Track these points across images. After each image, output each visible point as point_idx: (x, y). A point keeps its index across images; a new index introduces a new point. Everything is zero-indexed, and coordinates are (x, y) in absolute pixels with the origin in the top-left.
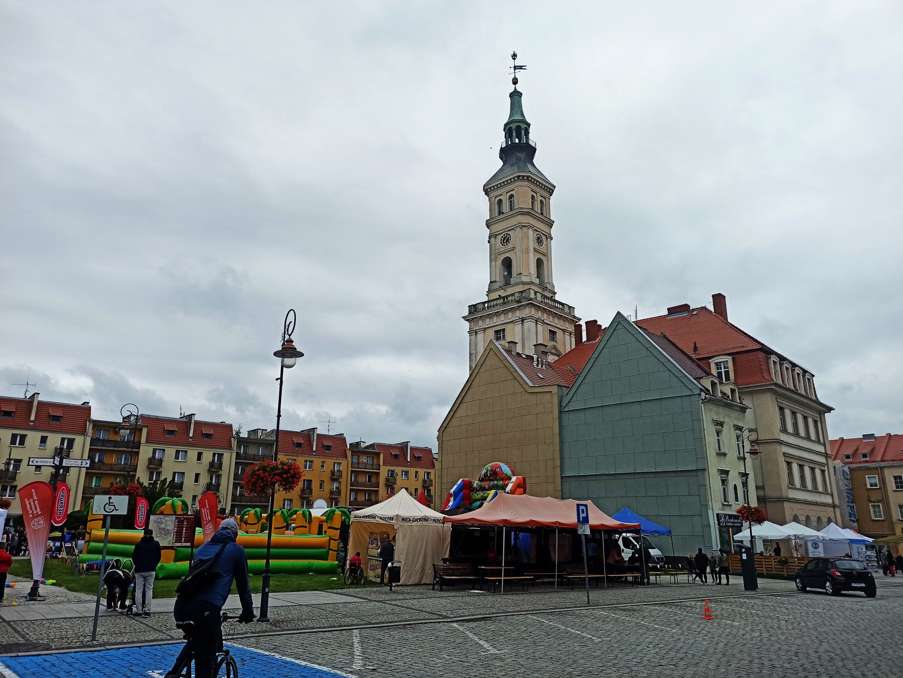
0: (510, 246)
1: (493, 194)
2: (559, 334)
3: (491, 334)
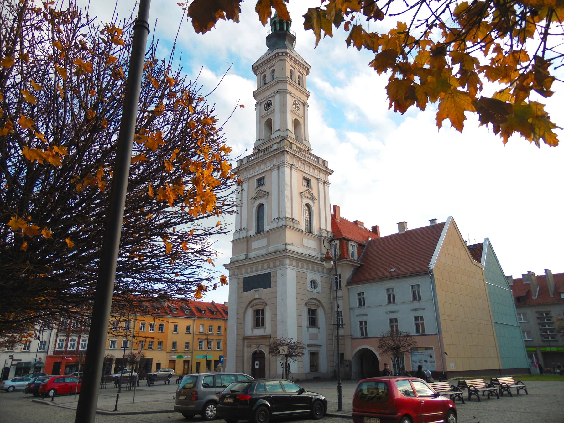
0: (271, 109)
1: (258, 72)
2: (314, 182)
3: (254, 182)
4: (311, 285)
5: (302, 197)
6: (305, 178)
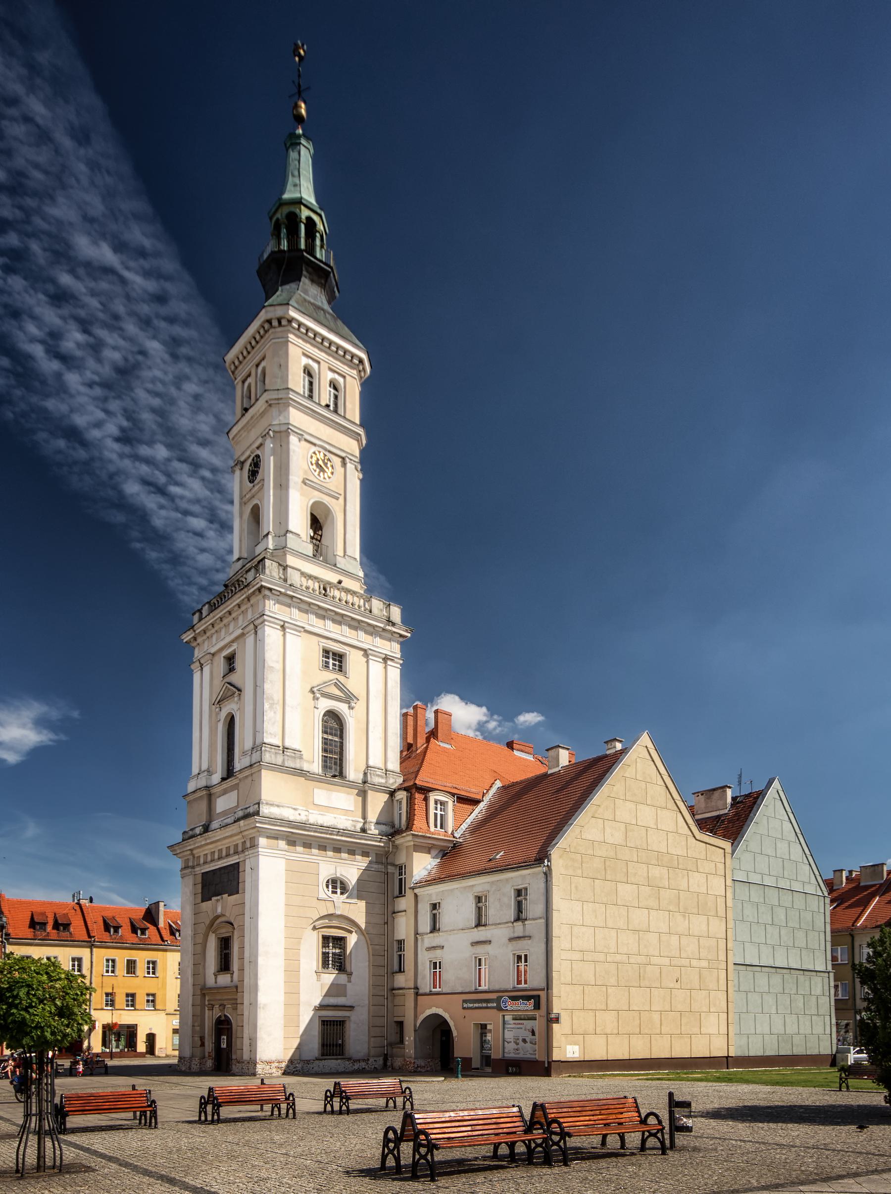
0: (259, 477)
4: (334, 887)
5: (315, 699)
6: (326, 652)
